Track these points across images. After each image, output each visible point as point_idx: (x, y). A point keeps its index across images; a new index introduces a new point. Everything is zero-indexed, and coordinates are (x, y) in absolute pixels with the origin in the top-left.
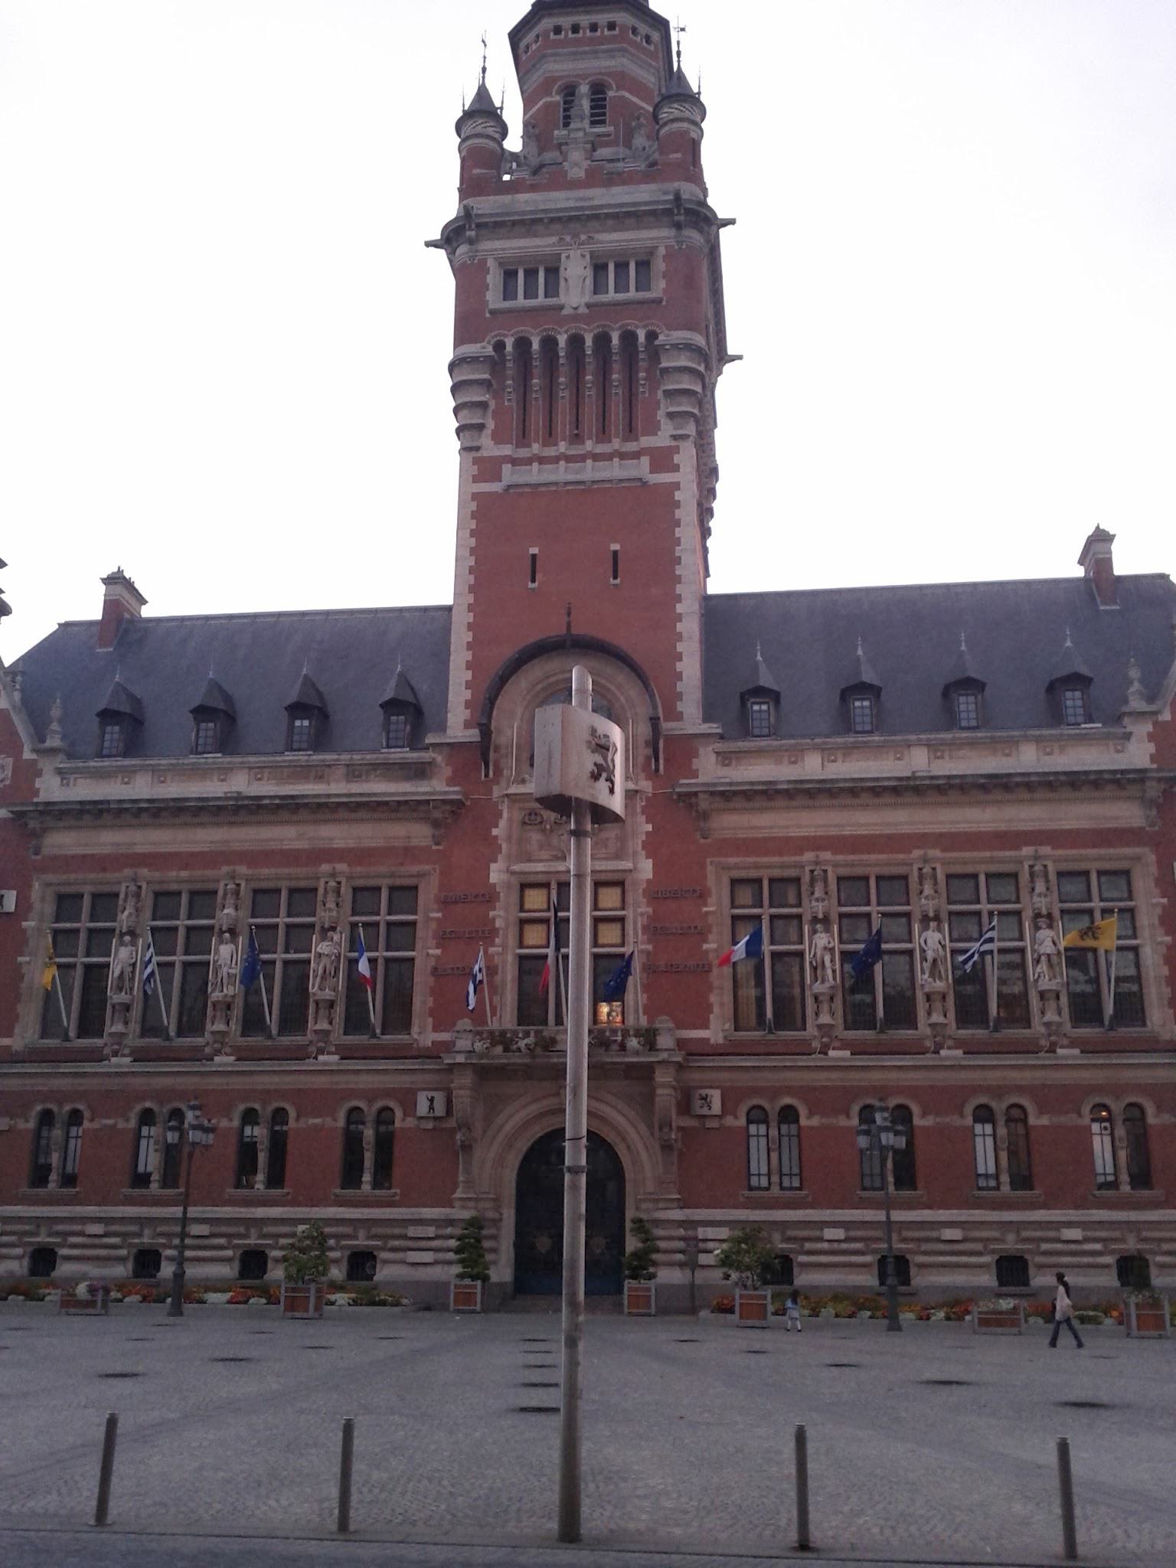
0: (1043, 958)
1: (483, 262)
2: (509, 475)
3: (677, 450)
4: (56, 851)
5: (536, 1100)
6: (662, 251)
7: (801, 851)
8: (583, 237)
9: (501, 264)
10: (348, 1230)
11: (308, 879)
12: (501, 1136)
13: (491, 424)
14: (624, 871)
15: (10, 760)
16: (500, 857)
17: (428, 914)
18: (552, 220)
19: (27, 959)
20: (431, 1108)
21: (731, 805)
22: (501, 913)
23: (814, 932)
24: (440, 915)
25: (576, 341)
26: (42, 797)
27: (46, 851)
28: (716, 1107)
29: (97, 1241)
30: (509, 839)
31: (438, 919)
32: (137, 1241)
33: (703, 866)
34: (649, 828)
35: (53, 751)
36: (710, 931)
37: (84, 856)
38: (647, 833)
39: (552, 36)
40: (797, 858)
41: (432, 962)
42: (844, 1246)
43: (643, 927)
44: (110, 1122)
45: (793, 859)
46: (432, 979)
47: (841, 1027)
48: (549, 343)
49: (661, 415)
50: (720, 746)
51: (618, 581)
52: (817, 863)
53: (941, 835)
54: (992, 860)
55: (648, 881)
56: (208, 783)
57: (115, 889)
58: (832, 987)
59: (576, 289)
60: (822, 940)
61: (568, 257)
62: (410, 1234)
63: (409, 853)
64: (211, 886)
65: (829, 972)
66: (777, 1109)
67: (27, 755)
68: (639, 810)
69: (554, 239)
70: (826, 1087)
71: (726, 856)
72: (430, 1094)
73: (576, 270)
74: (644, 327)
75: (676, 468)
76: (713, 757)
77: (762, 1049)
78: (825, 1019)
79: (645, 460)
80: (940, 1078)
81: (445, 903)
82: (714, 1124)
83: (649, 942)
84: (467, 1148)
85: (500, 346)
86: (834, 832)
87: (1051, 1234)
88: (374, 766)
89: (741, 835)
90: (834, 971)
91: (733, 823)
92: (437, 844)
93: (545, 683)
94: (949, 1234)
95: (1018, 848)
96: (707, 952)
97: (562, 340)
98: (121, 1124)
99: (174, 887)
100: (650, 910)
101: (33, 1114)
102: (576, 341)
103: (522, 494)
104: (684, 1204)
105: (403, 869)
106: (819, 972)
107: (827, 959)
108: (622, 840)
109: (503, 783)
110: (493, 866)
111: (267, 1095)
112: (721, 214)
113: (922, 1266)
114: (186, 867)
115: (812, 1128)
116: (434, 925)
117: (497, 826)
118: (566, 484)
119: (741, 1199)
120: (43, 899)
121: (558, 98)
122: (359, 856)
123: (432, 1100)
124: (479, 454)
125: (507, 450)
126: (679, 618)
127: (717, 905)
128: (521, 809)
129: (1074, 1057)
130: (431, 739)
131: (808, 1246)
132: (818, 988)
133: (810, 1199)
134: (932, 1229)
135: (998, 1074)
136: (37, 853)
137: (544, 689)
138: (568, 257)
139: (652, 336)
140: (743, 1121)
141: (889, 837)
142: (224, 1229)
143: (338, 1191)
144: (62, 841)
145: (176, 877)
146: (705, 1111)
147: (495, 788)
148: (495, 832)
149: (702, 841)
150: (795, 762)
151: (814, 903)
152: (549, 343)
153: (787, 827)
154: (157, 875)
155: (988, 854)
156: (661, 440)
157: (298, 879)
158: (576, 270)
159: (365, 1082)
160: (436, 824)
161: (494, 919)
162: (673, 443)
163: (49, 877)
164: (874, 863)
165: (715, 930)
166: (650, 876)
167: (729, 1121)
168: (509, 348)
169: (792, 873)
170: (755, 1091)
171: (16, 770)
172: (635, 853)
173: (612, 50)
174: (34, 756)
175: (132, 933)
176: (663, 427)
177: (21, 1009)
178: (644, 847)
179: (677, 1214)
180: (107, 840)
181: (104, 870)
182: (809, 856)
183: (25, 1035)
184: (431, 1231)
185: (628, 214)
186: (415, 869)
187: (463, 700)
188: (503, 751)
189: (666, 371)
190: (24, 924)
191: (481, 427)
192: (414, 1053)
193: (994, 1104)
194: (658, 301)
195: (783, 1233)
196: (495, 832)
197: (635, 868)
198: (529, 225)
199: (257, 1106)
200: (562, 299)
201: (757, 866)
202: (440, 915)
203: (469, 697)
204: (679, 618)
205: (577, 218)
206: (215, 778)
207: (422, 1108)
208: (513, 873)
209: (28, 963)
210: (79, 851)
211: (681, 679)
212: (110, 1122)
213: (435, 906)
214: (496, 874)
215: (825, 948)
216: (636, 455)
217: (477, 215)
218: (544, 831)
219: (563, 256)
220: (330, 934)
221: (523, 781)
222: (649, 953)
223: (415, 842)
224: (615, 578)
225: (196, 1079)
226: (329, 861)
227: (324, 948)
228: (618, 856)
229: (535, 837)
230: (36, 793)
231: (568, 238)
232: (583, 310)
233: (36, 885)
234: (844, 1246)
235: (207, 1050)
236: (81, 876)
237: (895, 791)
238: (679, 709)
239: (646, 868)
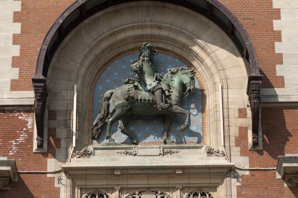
93: (112, 40)
137: (111, 47)
187: (9, 57)
188: (60, 118)
211: (280, 40)
221: (87, 154)
238: (279, 73)
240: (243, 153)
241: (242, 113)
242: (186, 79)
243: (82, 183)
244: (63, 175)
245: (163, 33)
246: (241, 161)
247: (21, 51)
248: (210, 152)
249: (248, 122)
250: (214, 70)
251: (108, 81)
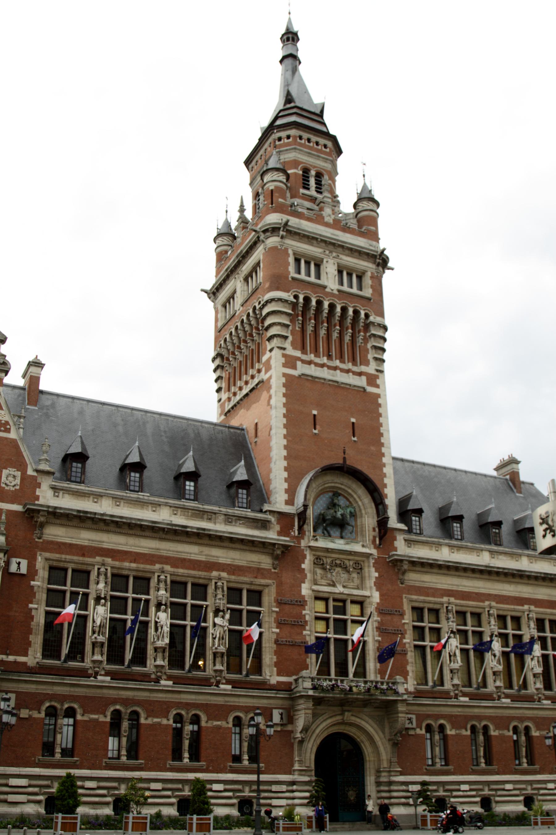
0: (536, 658)
1: (286, 250)
2: (301, 369)
3: (377, 377)
4: (50, 538)
5: (331, 717)
6: (369, 274)
7: (442, 596)
8: (334, 254)
9: (294, 254)
10: (239, 787)
11: (204, 579)
12: (314, 736)
13: (290, 338)
14: (366, 596)
15: (18, 474)
16: (306, 580)
17: (269, 607)
18: (322, 240)
19: (36, 606)
20: (282, 718)
21: (414, 568)
22: (308, 612)
24: (277, 610)
25: (332, 307)
26: (41, 501)
27: (46, 537)
28: (414, 725)
29: (92, 792)
30: (310, 571)
31: (276, 612)
32: (116, 792)
33: (402, 598)
34: (377, 575)
35: (48, 473)
36: (406, 633)
37: (71, 545)
38: (376, 578)
39: (298, 140)
40: (441, 600)
41: (274, 636)
42: (469, 793)
43: (377, 628)
44: (95, 716)
46: (275, 646)
48: (319, 303)
49: (370, 357)
50: (407, 536)
51: (355, 439)
53: (496, 595)
54: (514, 610)
55: (378, 604)
56: (145, 511)
57: (89, 568)
59: (330, 279)
61: (327, 262)
62: (273, 790)
63: (259, 572)
64: (148, 575)
66: (438, 725)
67: (30, 472)
68: (372, 564)
69: (320, 250)
70: (457, 715)
71: (411, 595)
72: (281, 711)
73: (330, 269)
74: (364, 310)
75: (378, 386)
76: (403, 542)
77: (430, 695)
78: (456, 681)
79: (364, 378)
80: (500, 712)
81: (280, 603)
82: (411, 732)
83: (379, 636)
84: (301, 742)
85: (296, 297)
86: (455, 588)
87: (544, 786)
88: (239, 518)
89: (417, 584)
91: (414, 578)
92: (275, 569)
94: (509, 786)
95: (523, 605)
96: (405, 644)
97: (326, 304)
98: (102, 719)
99: (125, 572)
100: (379, 619)
101: (44, 708)
102: (332, 307)
103: (307, 380)
104: (402, 774)
105: (256, 580)
106: (452, 658)
108: (362, 579)
109: (306, 538)
110: (303, 585)
111: (188, 706)
112: (390, 265)
113: (497, 802)
114: (135, 561)
115: (452, 735)
116: (274, 615)
117: (304, 563)
118: (330, 380)
119: (425, 771)
120: (44, 568)
121: (301, 172)
122: (232, 569)
123: (281, 714)
124: (284, 352)
125: (298, 354)
126: (384, 465)
127: (408, 619)
128: (314, 555)
129: (549, 705)
130: (266, 507)
131: (455, 793)
133: (452, 770)
134: (501, 784)
135: (521, 711)
136: (39, 538)
138: (327, 262)
139: (367, 316)
140: (423, 732)
141: (477, 594)
142: (170, 786)
143: (231, 764)
144: (56, 533)
145: (129, 566)
146: (410, 726)
147: (302, 541)
148: (303, 566)
149: (401, 585)
150: (437, 551)
152: (319, 303)
153: (436, 583)
154: (117, 564)
155: (512, 607)
156: (371, 369)
157: (200, 578)
158: (330, 269)
159: (243, 702)
160: (276, 558)
161: (305, 615)
162: (376, 373)
163: (48, 555)
164: (471, 605)
165: (408, 632)
166: (378, 601)
167: (418, 731)
168: (301, 300)
170: (428, 716)
171: (22, 479)
172: (371, 588)
173: (327, 159)
174: (35, 474)
175: (105, 598)
176: (371, 363)
177: (31, 638)
178: (375, 585)
179: (402, 778)
180: (86, 537)
181: (83, 555)
182: (445, 599)
183: (34, 656)
184: (284, 788)
185: (357, 251)
186: (263, 581)
189: (374, 335)
190: (32, 583)
191: (286, 338)
192: (267, 687)
193: (520, 726)
194: (369, 299)
195: (444, 787)
196: (303, 566)
197: (372, 596)
198: (310, 238)
199: (183, 712)
200: (323, 281)
201: (424, 602)
202: (277, 610)
203: (287, 487)
204: (384, 465)
205: (334, 244)
206: (150, 508)
207: (276, 718)
208: (313, 591)
209: (36, 609)
210: (68, 541)
212: (95, 716)
213: (275, 604)
214: (306, 590)
216: (360, 374)
217: (290, 226)
218: (324, 569)
219: (325, 260)
220: (221, 614)
221: (316, 540)
222: (379, 642)
223: (263, 566)
224: (354, 437)
225: (146, 694)
226: (218, 570)
227: (218, 620)
228: (358, 588)
229: (319, 571)
230: (38, 498)
231: (327, 252)
232: (336, 292)
233: (39, 558)
234: (469, 793)
235: (153, 676)
236: (68, 557)
237: (481, 572)
239: (376, 597)
240: (375, 548)
241: (374, 530)
242: (353, 510)
243: (314, 553)
244: (308, 548)
245: (343, 487)
246: (374, 552)
247: (288, 486)
248: (363, 546)
249: (376, 533)
250: (362, 507)
251: (319, 505)
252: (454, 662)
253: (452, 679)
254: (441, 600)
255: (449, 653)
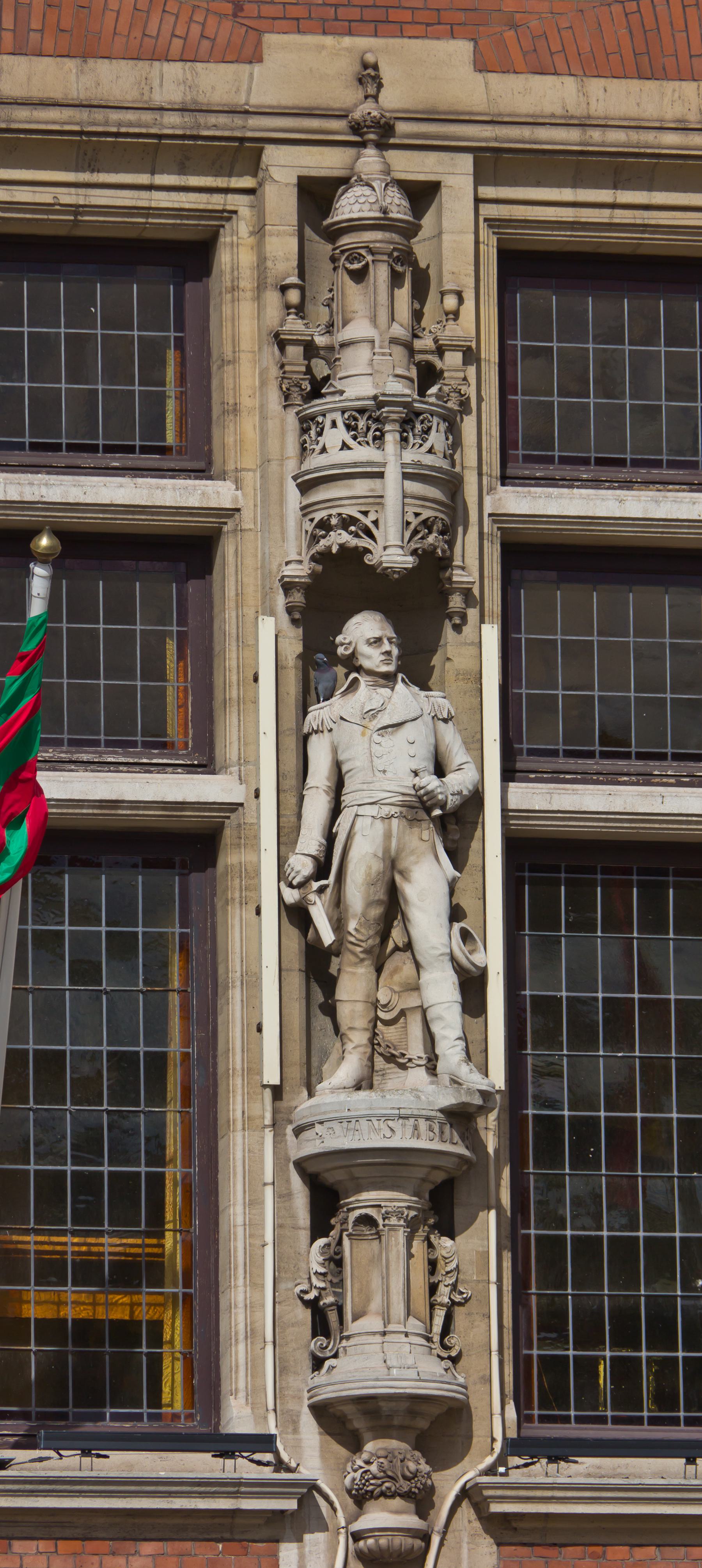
23: (320, 666)
40: (218, 82)
45: (170, 81)
47: (496, 1418)
52: (380, 133)
58: (461, 1118)
60: (391, 737)
65: (441, 991)
90: (472, 986)
106: (353, 985)
107: (426, 884)
132: (350, 1112)
151: (336, 446)
169: (167, 197)
215: (419, 806)
252: (383, 1056)
253: (324, 1321)
254: (218, 82)
255: (297, 916)
